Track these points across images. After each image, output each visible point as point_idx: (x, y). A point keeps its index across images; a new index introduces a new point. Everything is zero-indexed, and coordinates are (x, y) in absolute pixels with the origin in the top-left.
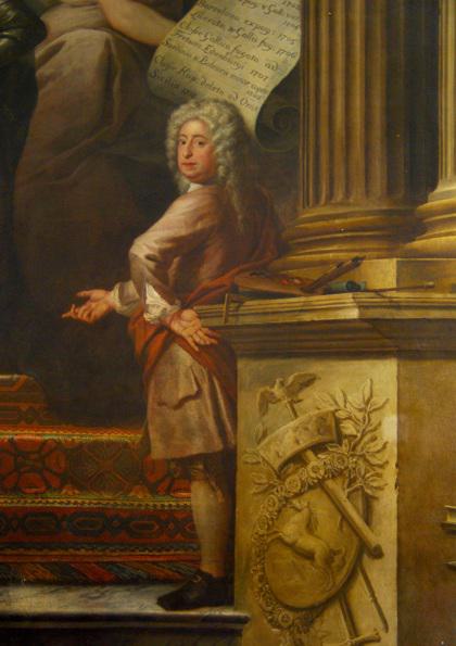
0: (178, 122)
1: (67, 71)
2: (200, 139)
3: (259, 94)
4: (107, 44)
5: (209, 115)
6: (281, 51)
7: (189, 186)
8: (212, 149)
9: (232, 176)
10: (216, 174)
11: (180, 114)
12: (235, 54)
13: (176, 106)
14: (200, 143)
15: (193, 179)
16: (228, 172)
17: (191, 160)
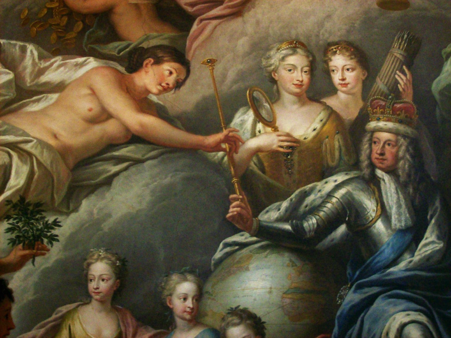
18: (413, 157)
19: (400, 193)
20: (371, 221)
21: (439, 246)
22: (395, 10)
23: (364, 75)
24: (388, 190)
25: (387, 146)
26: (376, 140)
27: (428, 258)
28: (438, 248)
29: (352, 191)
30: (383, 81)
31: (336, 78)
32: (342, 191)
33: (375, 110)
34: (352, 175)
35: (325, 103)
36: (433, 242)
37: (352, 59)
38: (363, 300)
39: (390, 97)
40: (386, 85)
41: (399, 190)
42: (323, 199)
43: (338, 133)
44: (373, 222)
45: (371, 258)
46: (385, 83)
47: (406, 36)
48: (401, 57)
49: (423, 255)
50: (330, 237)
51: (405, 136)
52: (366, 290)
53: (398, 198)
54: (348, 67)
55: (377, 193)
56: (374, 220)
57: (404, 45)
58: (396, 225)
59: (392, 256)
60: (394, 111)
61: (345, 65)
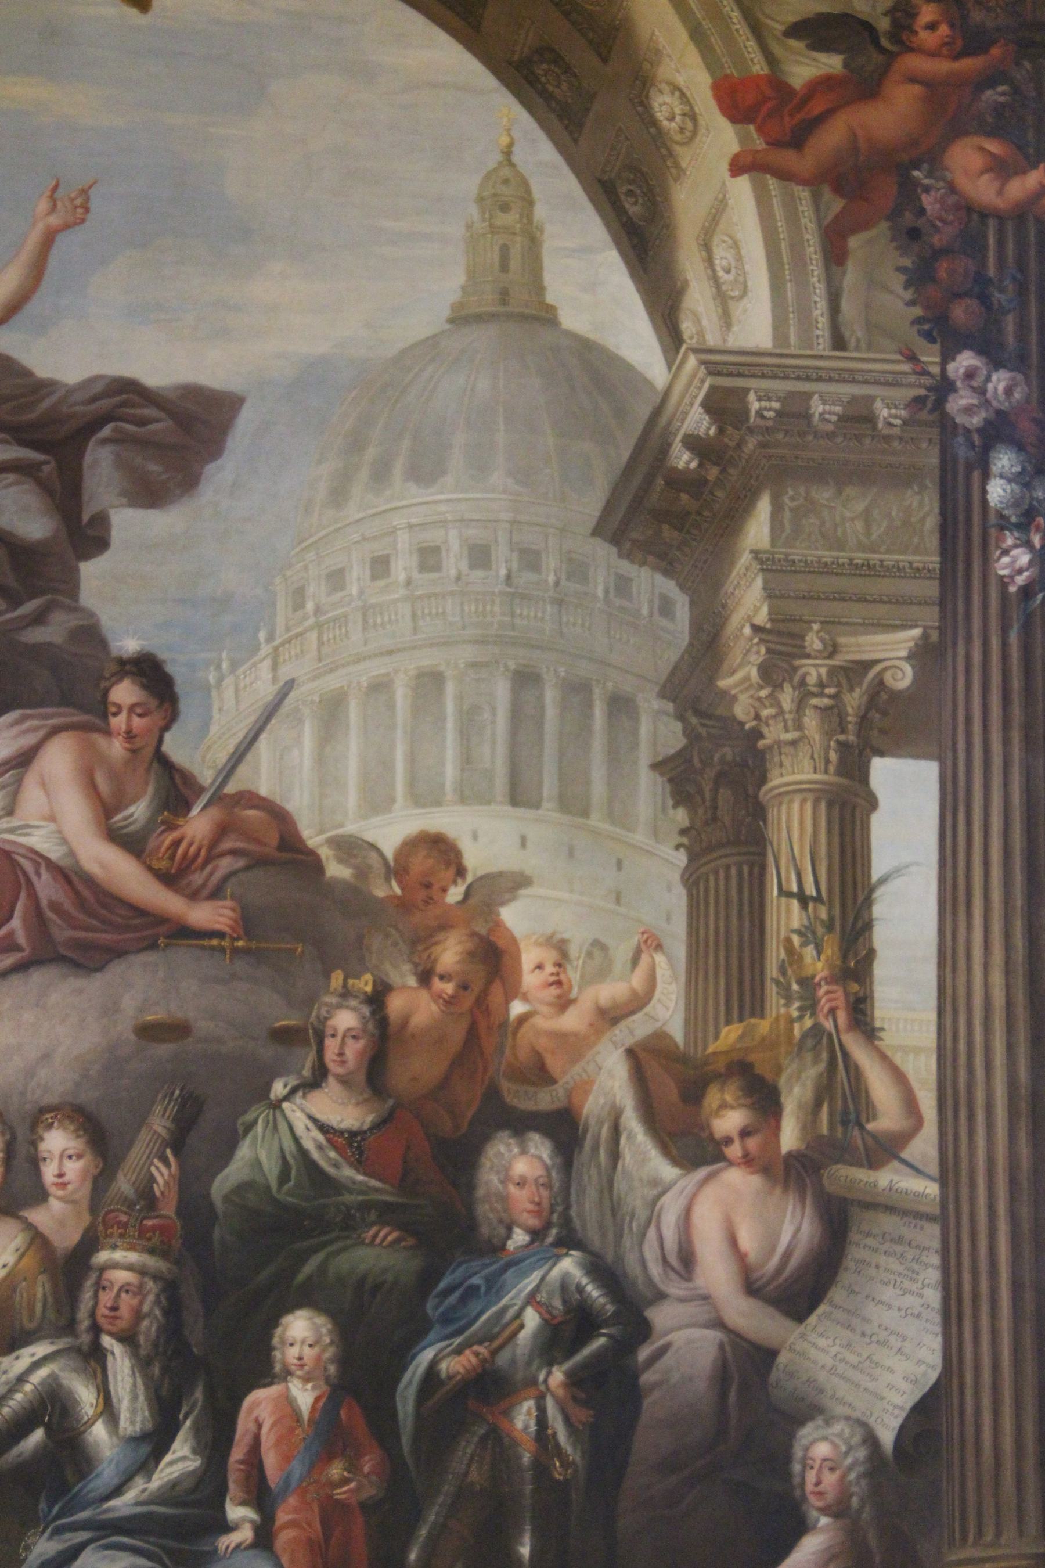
0: (804, 1442)
1: (675, 1377)
2: (829, 1464)
3: (896, 1412)
4: (721, 1346)
5: (840, 1435)
6: (920, 1362)
7: (817, 1520)
8: (843, 1477)
9: (867, 1509)
10: (849, 1507)
11: (806, 1433)
12: (868, 1362)
13: (802, 1423)
14: (832, 1469)
15: (824, 1511)
16: (863, 1502)
17: (821, 1488)
18: (166, 1313)
19: (137, 1375)
20: (86, 1423)
21: (194, 1464)
22: (163, 1041)
23: (97, 1167)
24: (119, 1369)
25: (123, 1295)
26: (105, 1283)
27: (174, 1485)
28: (191, 1469)
29: (57, 1371)
30: (128, 1177)
31: (49, 1172)
32: (43, 1372)
33: (110, 1231)
34: (61, 1344)
35: (26, 1218)
36: (184, 1458)
37: (78, 1137)
38: (60, 1553)
39: (138, 1207)
40: (134, 1183)
41: (136, 1370)
42: (11, 1385)
43: (44, 1271)
44: (88, 1425)
45: (80, 1485)
46: (132, 1182)
47: (177, 1092)
48: (164, 1133)
49: (166, 1479)
50: (15, 1451)
51: (156, 1277)
52: (68, 1535)
53: (135, 1385)
54: (71, 1152)
55: (99, 1375)
56: (91, 1421)
57: (173, 1109)
58: (125, 1429)
59: (116, 1481)
60: (142, 1232)
61: (66, 1149)
